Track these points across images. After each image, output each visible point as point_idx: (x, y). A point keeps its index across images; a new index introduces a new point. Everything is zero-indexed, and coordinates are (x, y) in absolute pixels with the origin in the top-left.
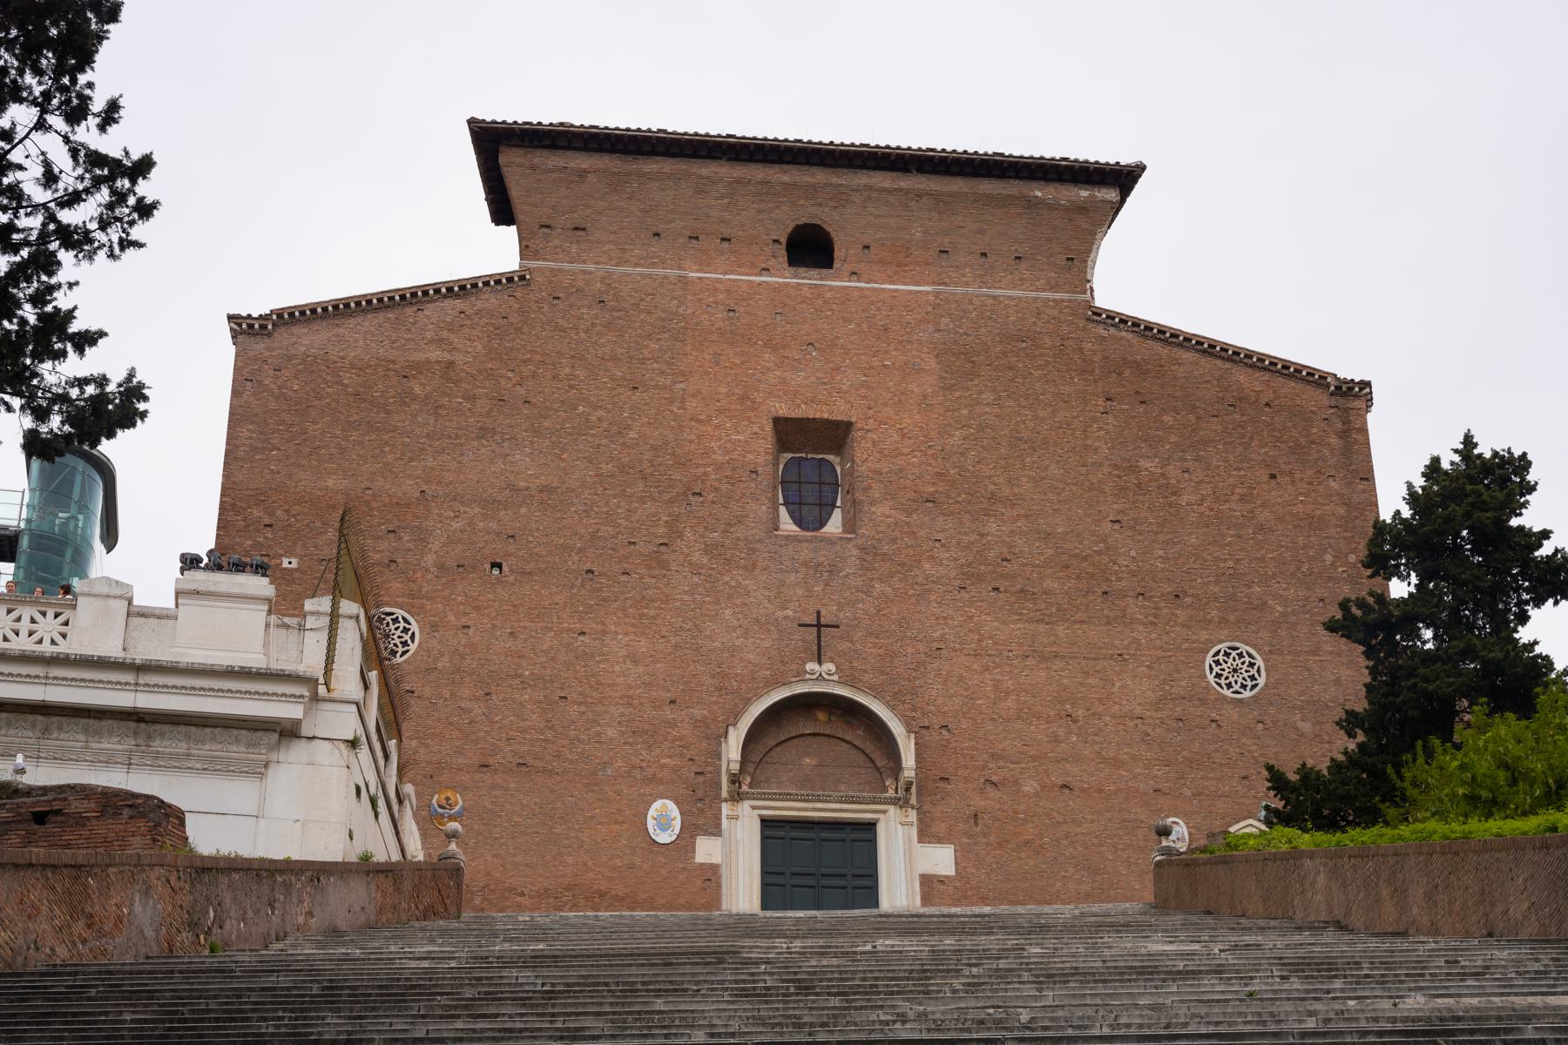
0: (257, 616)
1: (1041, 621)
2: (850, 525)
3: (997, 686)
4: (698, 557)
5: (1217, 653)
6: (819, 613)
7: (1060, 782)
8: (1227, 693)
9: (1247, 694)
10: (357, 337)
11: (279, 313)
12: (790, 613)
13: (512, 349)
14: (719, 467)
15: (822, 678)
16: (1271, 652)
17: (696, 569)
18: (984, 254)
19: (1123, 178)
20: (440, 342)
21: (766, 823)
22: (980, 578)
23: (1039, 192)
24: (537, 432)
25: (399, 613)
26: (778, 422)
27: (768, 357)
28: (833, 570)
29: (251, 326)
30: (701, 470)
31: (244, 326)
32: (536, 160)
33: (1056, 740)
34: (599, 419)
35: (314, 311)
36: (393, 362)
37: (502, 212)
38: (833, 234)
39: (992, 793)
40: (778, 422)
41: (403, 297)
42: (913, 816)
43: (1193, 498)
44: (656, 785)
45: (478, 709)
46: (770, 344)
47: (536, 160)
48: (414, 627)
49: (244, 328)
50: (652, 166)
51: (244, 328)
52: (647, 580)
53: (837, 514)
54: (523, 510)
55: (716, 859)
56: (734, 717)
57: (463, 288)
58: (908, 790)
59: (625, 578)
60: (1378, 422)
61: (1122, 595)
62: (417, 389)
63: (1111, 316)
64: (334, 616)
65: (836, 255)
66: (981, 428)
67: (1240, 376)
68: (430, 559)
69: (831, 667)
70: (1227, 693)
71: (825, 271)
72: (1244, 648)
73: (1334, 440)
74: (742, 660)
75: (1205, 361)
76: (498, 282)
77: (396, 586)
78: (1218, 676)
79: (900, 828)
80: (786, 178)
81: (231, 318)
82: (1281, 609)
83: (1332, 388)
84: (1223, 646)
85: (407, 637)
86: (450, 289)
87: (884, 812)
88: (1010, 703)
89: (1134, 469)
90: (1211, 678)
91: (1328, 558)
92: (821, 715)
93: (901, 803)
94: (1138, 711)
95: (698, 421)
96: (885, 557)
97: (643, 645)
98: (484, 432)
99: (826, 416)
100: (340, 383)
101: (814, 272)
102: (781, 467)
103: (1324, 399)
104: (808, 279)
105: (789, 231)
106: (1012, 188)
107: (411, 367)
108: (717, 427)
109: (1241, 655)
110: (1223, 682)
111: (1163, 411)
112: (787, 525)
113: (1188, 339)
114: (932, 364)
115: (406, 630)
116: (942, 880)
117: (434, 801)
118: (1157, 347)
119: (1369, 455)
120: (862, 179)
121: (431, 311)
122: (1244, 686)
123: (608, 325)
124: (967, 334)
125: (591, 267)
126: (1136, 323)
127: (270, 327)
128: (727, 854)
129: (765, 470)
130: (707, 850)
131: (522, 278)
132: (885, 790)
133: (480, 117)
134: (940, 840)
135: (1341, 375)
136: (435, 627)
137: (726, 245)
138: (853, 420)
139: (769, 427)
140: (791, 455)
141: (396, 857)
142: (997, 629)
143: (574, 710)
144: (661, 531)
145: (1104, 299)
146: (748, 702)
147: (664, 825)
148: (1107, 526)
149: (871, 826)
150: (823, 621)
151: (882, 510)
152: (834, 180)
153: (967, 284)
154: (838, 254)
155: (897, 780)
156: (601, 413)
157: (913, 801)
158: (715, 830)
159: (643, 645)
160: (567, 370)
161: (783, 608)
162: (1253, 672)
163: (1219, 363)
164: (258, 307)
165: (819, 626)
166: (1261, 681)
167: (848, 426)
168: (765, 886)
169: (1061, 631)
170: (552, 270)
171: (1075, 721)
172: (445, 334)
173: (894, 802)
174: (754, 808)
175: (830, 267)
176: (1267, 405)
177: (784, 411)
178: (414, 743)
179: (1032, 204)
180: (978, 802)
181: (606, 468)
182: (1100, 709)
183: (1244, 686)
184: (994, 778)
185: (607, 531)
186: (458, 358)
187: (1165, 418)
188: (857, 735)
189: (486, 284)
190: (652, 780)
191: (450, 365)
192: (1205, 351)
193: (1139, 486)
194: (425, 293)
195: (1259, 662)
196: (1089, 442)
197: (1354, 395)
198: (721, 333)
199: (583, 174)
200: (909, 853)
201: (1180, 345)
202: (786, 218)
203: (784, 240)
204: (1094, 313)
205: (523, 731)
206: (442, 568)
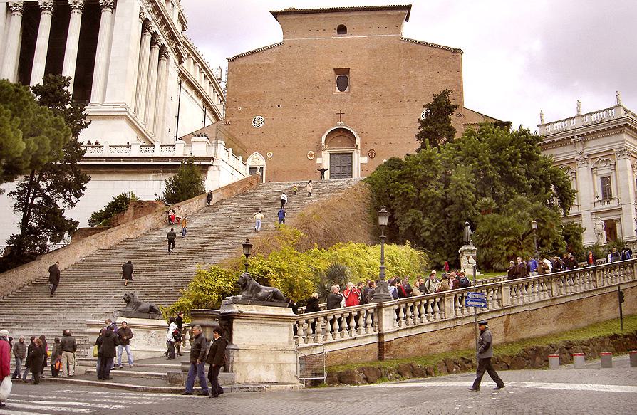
15: (340, 125)
19: (408, 8)
22: (375, 100)
42: (359, 151)
45: (275, 135)
50: (308, 16)
60: (463, 57)
64: (217, 144)
67: (434, 50)
75: (425, 47)
77: (260, 112)
93: (357, 149)
97: (307, 120)
98: (276, 78)
104: (341, 37)
114: (367, 53)
120: (351, 14)
123: (300, 52)
139: (333, 70)
145: (404, 36)
146: (327, 130)
147: (311, 156)
149: (351, 153)
159: (307, 120)
169: (391, 110)
173: (356, 149)
179: (388, 15)
200: (358, 159)
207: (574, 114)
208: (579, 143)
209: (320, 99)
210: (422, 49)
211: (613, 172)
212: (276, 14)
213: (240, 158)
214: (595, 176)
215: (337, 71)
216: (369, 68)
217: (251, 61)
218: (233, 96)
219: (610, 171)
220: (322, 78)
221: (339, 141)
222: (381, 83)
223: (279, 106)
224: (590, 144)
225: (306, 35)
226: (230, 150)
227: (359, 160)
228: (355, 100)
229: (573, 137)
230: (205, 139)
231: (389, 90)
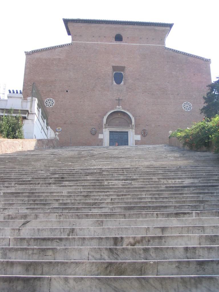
0: (20, 100)
1: (156, 99)
2: (124, 84)
5: (184, 104)
6: (119, 98)
7: (158, 125)
8: (186, 110)
9: (189, 110)
11: (32, 51)
12: (114, 98)
13: (70, 56)
15: (119, 108)
16: (193, 103)
18: (147, 39)
19: (170, 26)
21: (110, 132)
23: (157, 28)
25: (52, 99)
26: (113, 67)
29: (28, 53)
30: (100, 75)
31: (27, 53)
32: (74, 25)
34: (84, 67)
35: (38, 50)
36: (51, 58)
37: (69, 34)
38: (122, 36)
40: (113, 67)
41: (52, 48)
42: (134, 131)
47: (74, 25)
48: (54, 101)
49: (28, 54)
50: (93, 25)
51: (28, 54)
52: (92, 93)
53: (123, 82)
54: (71, 82)
55: (102, 138)
56: (105, 115)
57: (62, 46)
58: (133, 126)
59: (88, 93)
62: (55, 63)
63: (168, 49)
65: (123, 39)
69: (121, 107)
70: (186, 110)
71: (121, 42)
72: (189, 103)
73: (204, 69)
74: (107, 105)
76: (68, 45)
77: (51, 95)
78: (184, 107)
79: (132, 133)
80: (115, 27)
81: (25, 52)
82: (195, 96)
83: (204, 60)
84: (185, 103)
85: (53, 103)
86: (60, 46)
87: (129, 130)
90: (183, 108)
91: (203, 88)
92: (119, 114)
93: (132, 128)
95: (100, 67)
99: (121, 65)
100: (42, 62)
101: (119, 42)
102: (114, 74)
103: (203, 62)
104: (118, 43)
105: (115, 35)
106: (152, 27)
107: (54, 59)
108: (103, 68)
109: (188, 104)
110: (185, 108)
112: (115, 83)
113: (181, 52)
115: (53, 102)
116: (138, 141)
117: (57, 129)
118: (176, 53)
119: (210, 71)
120: (127, 26)
121: (57, 50)
122: (189, 109)
124: (144, 52)
125: (83, 42)
126: (172, 50)
127: (31, 53)
128: (103, 137)
130: (101, 136)
131: (71, 44)
133: (64, 18)
135: (206, 58)
136: (57, 101)
137: (105, 38)
138: (125, 66)
139: (112, 68)
140: (115, 72)
141: (47, 138)
142: (148, 100)
144: (94, 85)
146: (107, 112)
149: (127, 132)
150: (120, 99)
151: (130, 81)
152: (122, 27)
153: (144, 44)
154: (123, 39)
155: (131, 125)
156: (84, 66)
158: (102, 133)
160: (79, 59)
161: (113, 97)
162: (190, 107)
163: (186, 56)
164: (29, 50)
165: (119, 100)
166: (191, 108)
167: (125, 67)
168: (110, 142)
170: (76, 43)
171: (161, 115)
172: (59, 54)
174: (108, 129)
175: (122, 41)
176: (194, 63)
177: (114, 65)
178: (54, 120)
180: (145, 128)
181: (85, 75)
182: (165, 113)
183: (189, 109)
184: (147, 124)
186: (61, 57)
187: (177, 65)
189: (66, 45)
191: (60, 59)
192: (184, 54)
193: (172, 76)
194: (56, 47)
195: (191, 105)
196: (164, 69)
197: (208, 61)
199: (81, 27)
201: (179, 53)
202: (115, 33)
203: (114, 37)
204: (166, 48)
205: (71, 118)
206: (58, 91)
212: (67, 22)
215: (114, 68)
217: (45, 55)
221: (117, 122)
223: (67, 91)
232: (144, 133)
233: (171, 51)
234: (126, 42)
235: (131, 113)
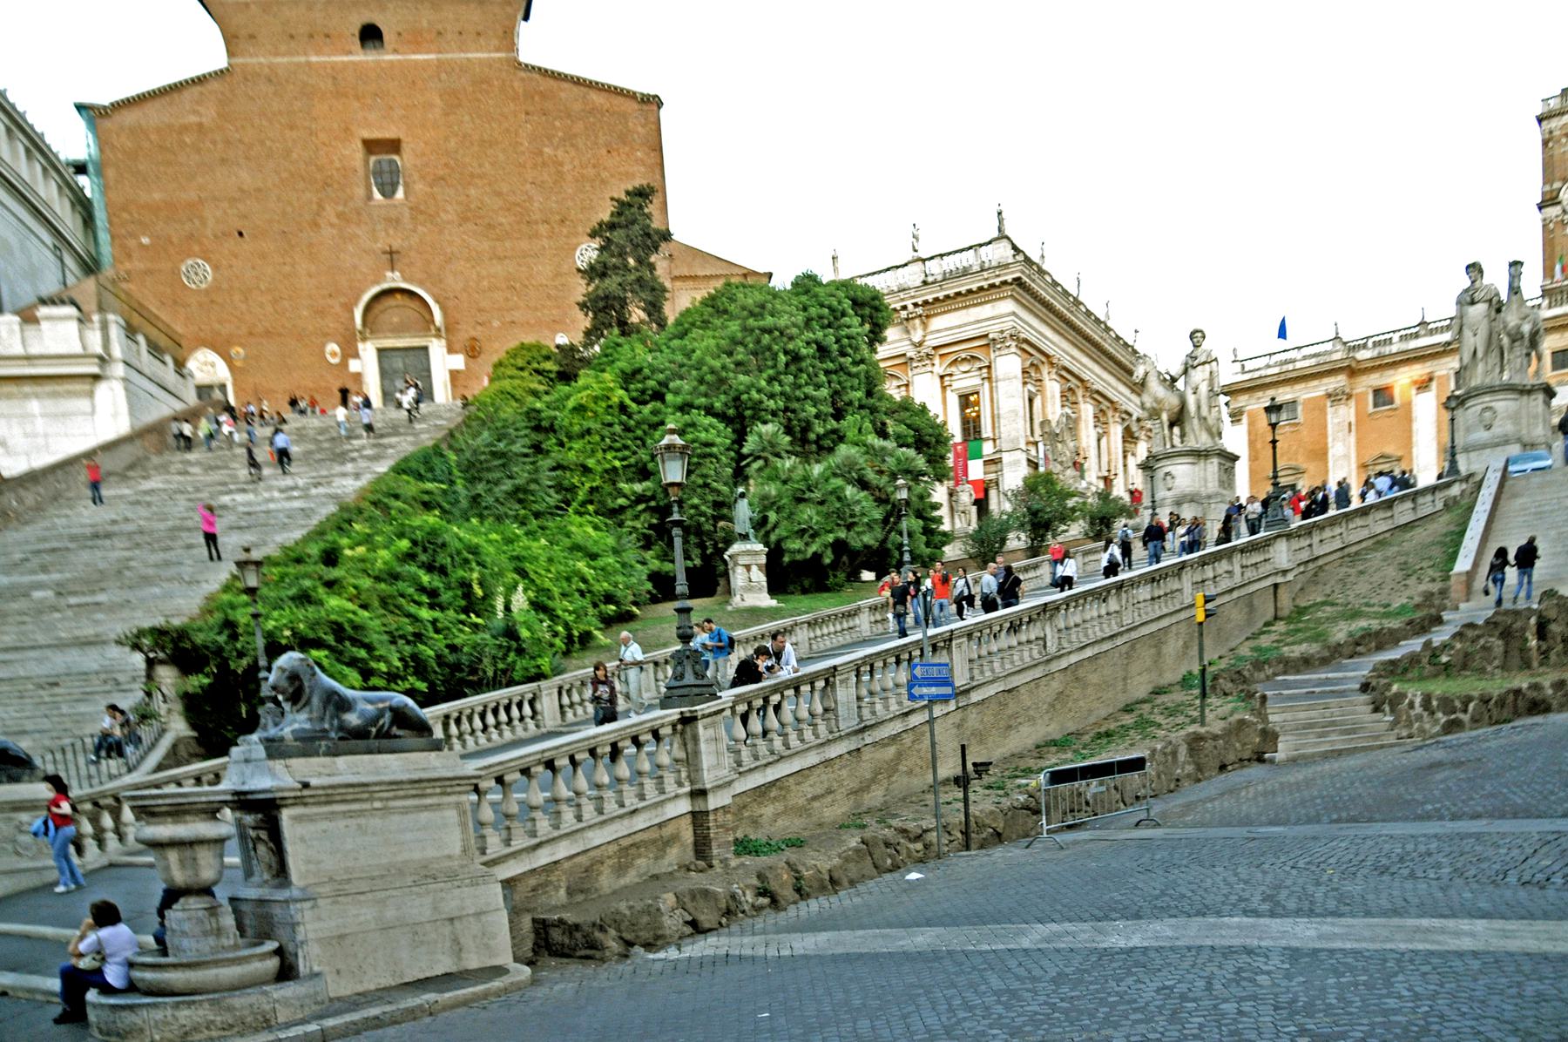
3: (478, 274)
4: (334, 220)
10: (152, 115)
14: (338, 169)
15: (394, 280)
17: (332, 225)
20: (196, 112)
21: (381, 351)
24: (247, 158)
27: (356, 104)
28: (398, 221)
33: (507, 300)
39: (479, 328)
42: (443, 342)
43: (570, 167)
44: (327, 336)
45: (243, 307)
46: (357, 98)
56: (356, 303)
60: (664, 113)
61: (536, 223)
62: (187, 140)
63: (526, 65)
66: (464, 137)
68: (209, 232)
75: (575, 89)
77: (196, 248)
88: (485, 283)
89: (541, 153)
93: (438, 336)
94: (545, 282)
96: (422, 212)
97: (313, 268)
98: (223, 161)
103: (635, 106)
111: (555, 119)
112: (377, 195)
114: (438, 101)
116: (458, 372)
118: (551, 82)
121: (187, 94)
125: (262, 60)
128: (363, 366)
129: (361, 172)
132: (429, 330)
134: (456, 352)
139: (360, 145)
143: (286, 304)
145: (524, 58)
146: (362, 292)
148: (528, 186)
149: (425, 349)
151: (419, 187)
154: (386, 37)
157: (443, 334)
158: (356, 356)
159: (313, 268)
169: (508, 244)
177: (367, 135)
180: (473, 333)
185: (289, 209)
187: (557, 123)
188: (415, 304)
190: (326, 335)
198: (331, 92)
206: (216, 236)
207: (910, 255)
208: (917, 321)
209: (339, 215)
210: (567, 92)
211: (986, 384)
213: (168, 359)
214: (949, 390)
216: (447, 139)
218: (124, 208)
219: (977, 381)
220: (337, 164)
222: (480, 177)
223: (241, 234)
224: (937, 323)
225: (283, 48)
226: (141, 339)
227: (443, 362)
228: (421, 217)
229: (904, 308)
230: (70, 310)
231: (499, 194)
232: (473, 349)
233: (537, 76)
234: (395, 51)
235: (427, 291)
